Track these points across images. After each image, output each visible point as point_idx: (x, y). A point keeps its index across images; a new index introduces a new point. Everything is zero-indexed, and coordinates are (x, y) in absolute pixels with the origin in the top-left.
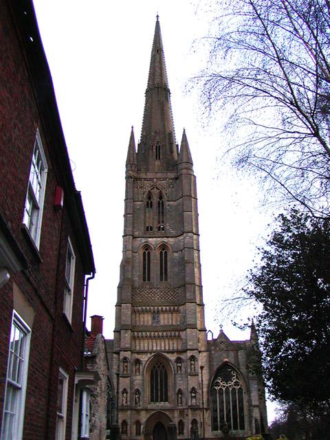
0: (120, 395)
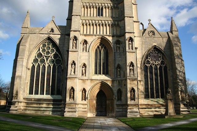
0: (69, 66)
